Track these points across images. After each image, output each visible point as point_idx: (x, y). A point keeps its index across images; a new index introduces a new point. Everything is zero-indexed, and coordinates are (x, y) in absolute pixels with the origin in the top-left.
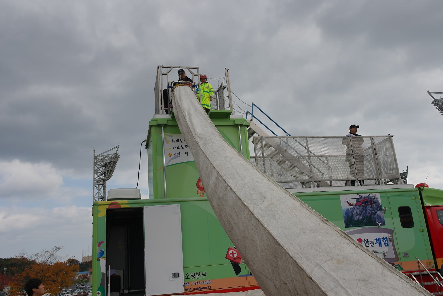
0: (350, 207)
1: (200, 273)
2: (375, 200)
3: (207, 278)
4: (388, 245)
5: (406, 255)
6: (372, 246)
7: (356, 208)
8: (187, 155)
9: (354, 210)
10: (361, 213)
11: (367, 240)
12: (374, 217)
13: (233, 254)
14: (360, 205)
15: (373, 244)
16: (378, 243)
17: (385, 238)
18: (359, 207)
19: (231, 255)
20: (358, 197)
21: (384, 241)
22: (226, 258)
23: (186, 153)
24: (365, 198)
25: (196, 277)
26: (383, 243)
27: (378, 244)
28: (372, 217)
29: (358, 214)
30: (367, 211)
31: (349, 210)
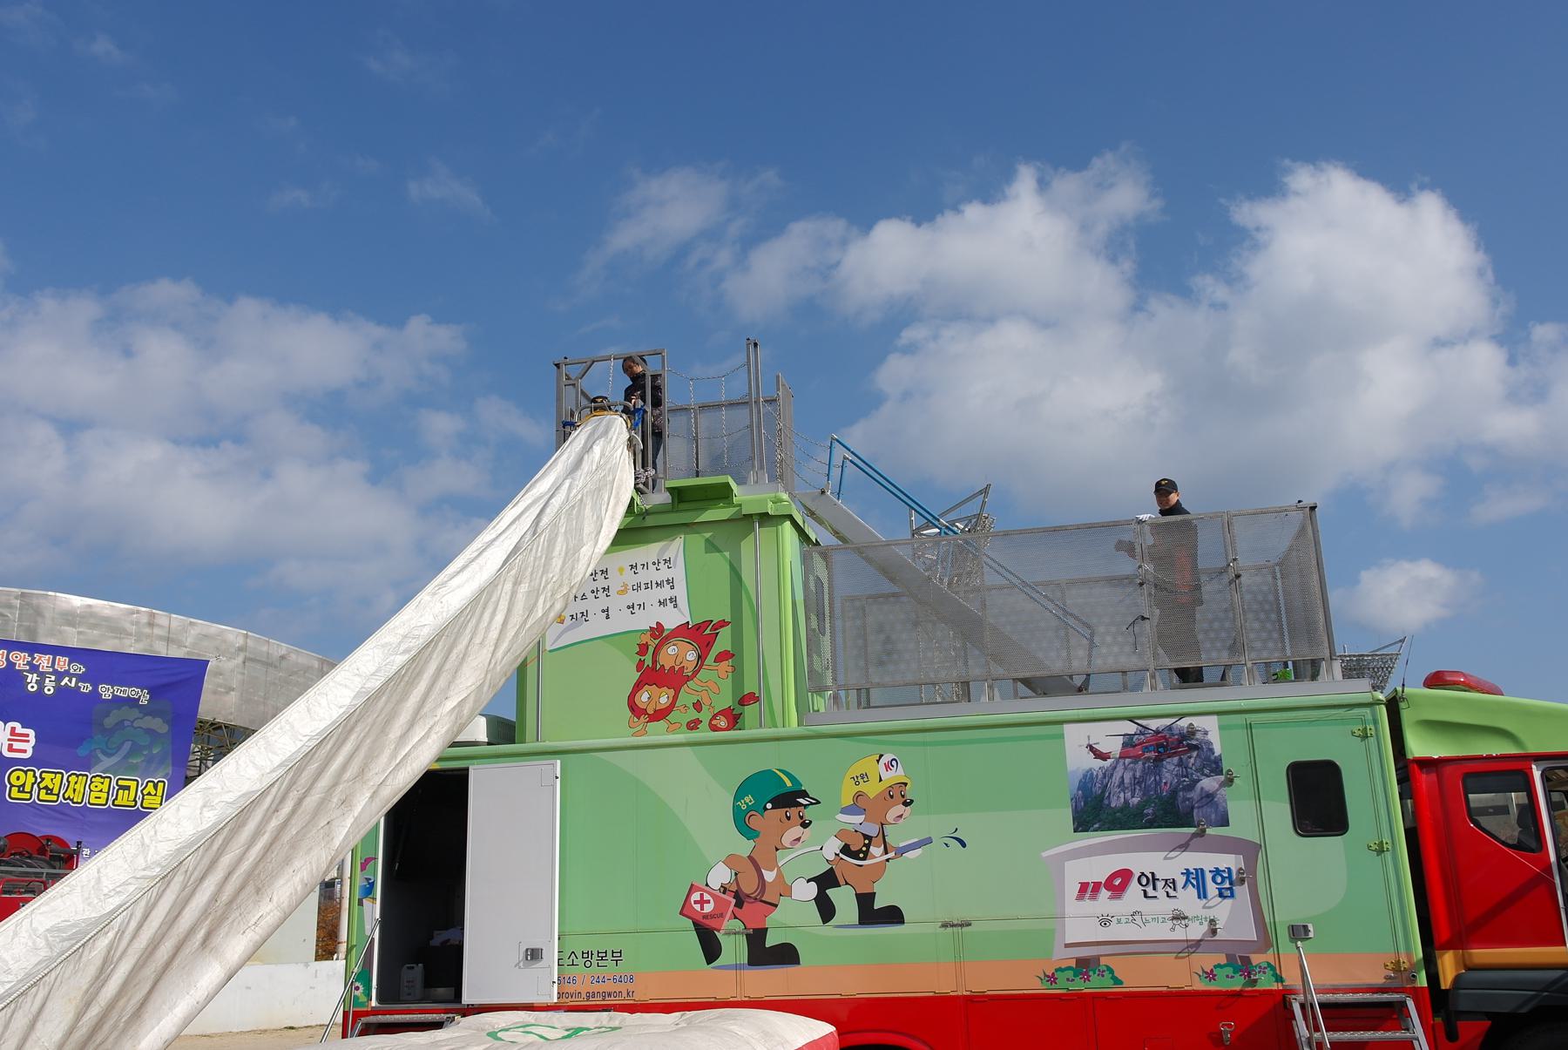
0: (1100, 763)
1: (606, 952)
2: (1197, 740)
3: (624, 968)
4: (1232, 896)
5: (1298, 933)
6: (1168, 896)
7: (1120, 768)
8: (608, 617)
9: (1112, 775)
10: (1139, 783)
11: (1153, 874)
12: (1188, 799)
13: (702, 902)
14: (1136, 758)
15: (1175, 890)
16: (1194, 886)
17: (1224, 871)
18: (1132, 765)
19: (697, 907)
20: (1131, 728)
21: (1219, 879)
22: (682, 913)
23: (603, 611)
24: (1157, 732)
25: (594, 962)
26: (1212, 889)
27: (1192, 891)
28: (1180, 799)
29: (1127, 788)
30: (1161, 779)
31: (1092, 774)
